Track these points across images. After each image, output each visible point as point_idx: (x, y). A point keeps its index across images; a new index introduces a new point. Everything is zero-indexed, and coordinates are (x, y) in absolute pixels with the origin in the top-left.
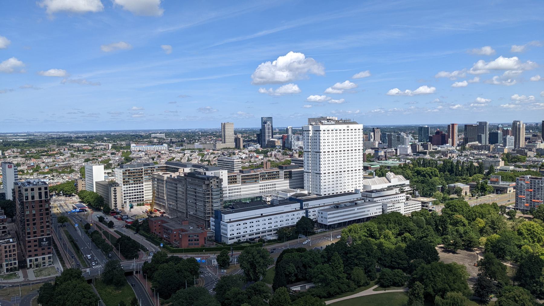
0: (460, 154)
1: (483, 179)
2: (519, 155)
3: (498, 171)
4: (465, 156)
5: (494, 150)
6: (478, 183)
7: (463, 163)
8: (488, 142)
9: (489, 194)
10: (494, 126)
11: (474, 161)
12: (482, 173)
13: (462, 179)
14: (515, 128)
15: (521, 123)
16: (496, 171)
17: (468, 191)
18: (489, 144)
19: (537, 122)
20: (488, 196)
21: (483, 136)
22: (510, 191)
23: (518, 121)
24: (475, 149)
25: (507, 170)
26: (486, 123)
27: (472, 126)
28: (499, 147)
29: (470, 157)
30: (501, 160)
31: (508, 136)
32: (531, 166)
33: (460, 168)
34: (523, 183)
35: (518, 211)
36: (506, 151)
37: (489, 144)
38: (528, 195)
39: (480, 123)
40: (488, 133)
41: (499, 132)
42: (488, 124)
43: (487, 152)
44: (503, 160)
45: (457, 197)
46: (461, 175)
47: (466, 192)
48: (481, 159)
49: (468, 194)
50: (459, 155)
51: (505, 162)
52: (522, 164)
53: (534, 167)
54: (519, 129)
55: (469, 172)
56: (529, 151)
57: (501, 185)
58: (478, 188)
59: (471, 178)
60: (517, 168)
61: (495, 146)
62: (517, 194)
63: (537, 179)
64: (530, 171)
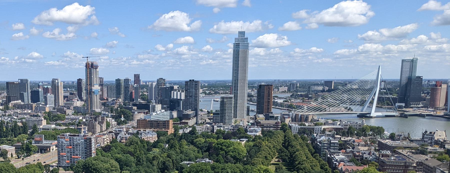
0: (4, 114)
1: (28, 139)
2: (59, 113)
3: (41, 130)
4: (9, 115)
5: (36, 108)
6: (23, 144)
7: (7, 123)
8: (30, 100)
9: (34, 154)
10: (35, 83)
11: (17, 120)
12: (26, 133)
13: (8, 141)
14: (54, 85)
15: (59, 81)
16: (40, 130)
17: (14, 152)
18: (32, 102)
19: (73, 80)
20: (33, 156)
21: (25, 94)
22: (53, 150)
23: (56, 79)
24: (18, 108)
25: (49, 129)
26: (27, 80)
27: (13, 83)
28: (41, 105)
29: (14, 117)
30: (43, 118)
31: (48, 94)
32: (69, 124)
33: (5, 129)
34: (63, 141)
35: (61, 168)
36: (47, 110)
37: (32, 102)
38: (68, 152)
39: (21, 80)
40: (29, 91)
41: (40, 90)
42: (29, 82)
43: (30, 111)
44: (45, 118)
45: (3, 160)
46: (6, 136)
47: (12, 154)
48: (24, 118)
49: (14, 156)
50: (3, 115)
51: (47, 121)
52: (62, 122)
53: (72, 124)
54: (58, 87)
55: (13, 133)
56: (68, 109)
57: (44, 144)
58: (23, 149)
59: (16, 139)
60: (58, 127)
61: (37, 104)
62: (59, 152)
63: (75, 136)
64: (69, 128)
